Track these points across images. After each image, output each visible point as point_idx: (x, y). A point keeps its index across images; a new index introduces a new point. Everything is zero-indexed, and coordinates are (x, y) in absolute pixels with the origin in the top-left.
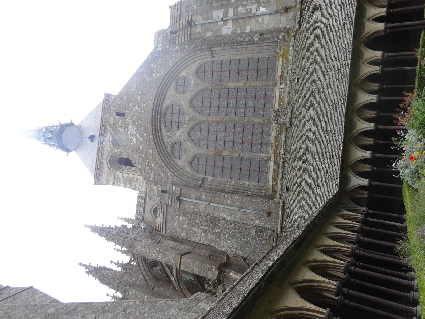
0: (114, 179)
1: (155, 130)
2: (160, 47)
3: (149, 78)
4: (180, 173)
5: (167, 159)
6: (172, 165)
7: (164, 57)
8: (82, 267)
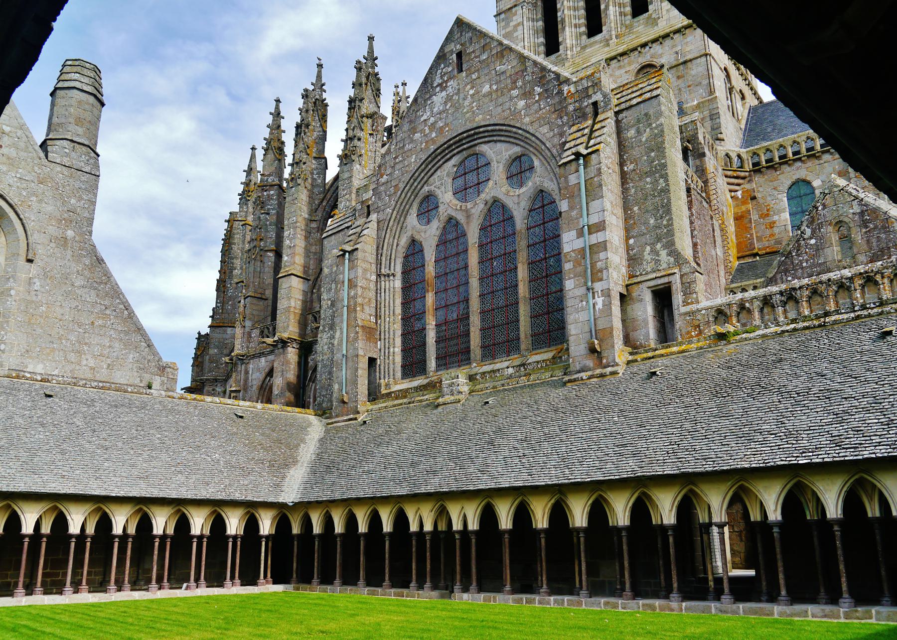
1: (444, 151)
2: (570, 91)
8: (315, 70)
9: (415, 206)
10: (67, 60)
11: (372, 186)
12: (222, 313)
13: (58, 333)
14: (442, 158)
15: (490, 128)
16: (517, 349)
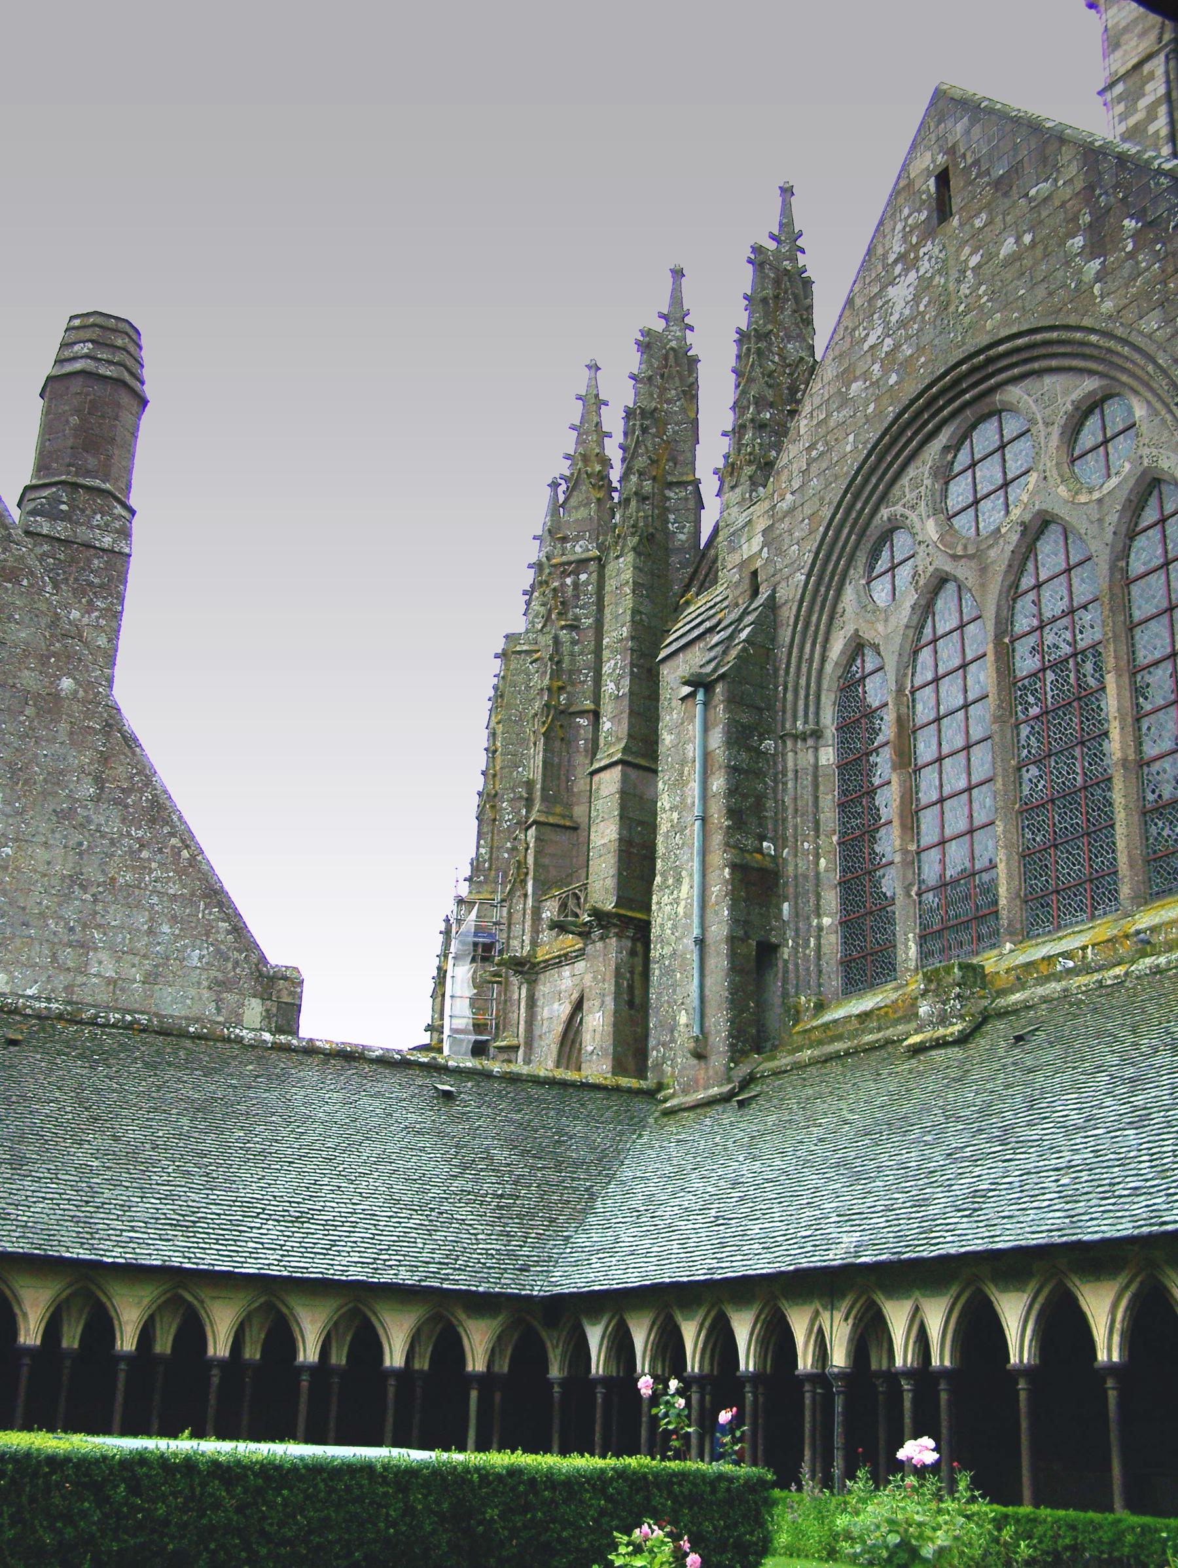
0: (1128, 72)
3: (1081, 244)
4: (814, 618)
5: (846, 531)
6: (830, 568)
7: (1170, 270)
9: (861, 559)
10: (72, 318)
11: (761, 524)
12: (490, 869)
13: (40, 903)
14: (916, 434)
15: (1020, 342)
16: (1114, 895)
